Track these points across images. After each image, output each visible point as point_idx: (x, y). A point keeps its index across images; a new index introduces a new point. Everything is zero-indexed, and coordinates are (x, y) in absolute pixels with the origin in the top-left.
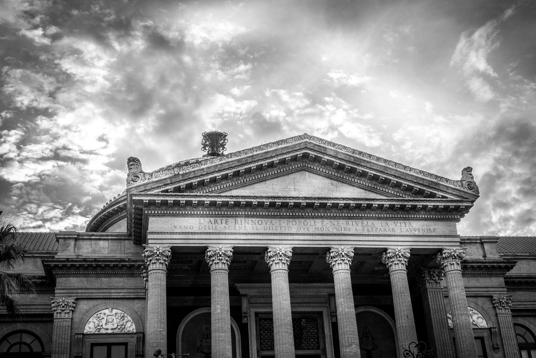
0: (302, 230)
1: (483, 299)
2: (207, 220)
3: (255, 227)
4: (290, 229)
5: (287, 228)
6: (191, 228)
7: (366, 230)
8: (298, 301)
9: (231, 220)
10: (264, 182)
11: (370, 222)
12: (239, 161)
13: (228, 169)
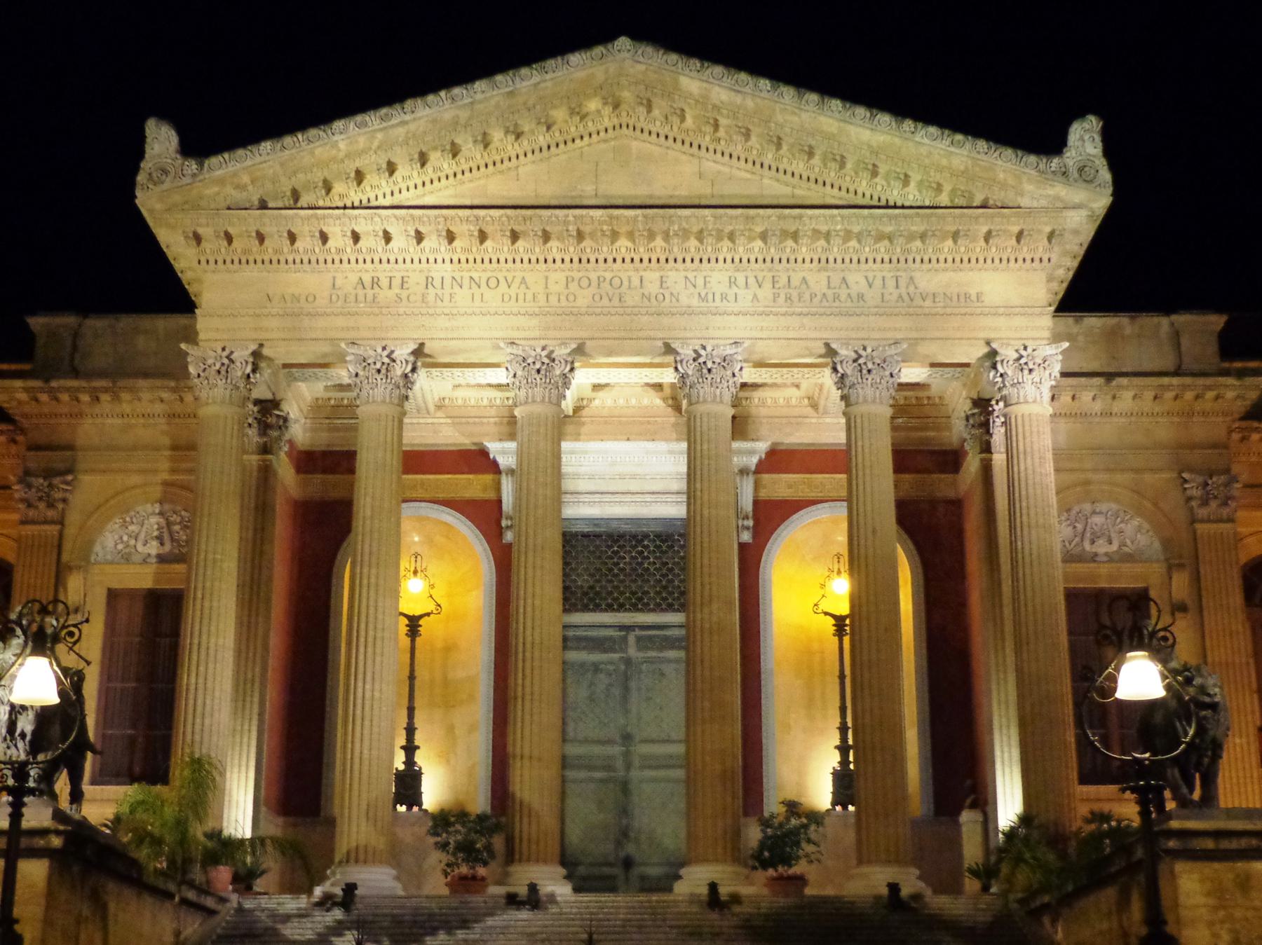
0: (605, 301)
3: (478, 298)
4: (571, 298)
5: (563, 298)
6: (311, 299)
7: (783, 296)
8: (654, 489)
10: (513, 173)
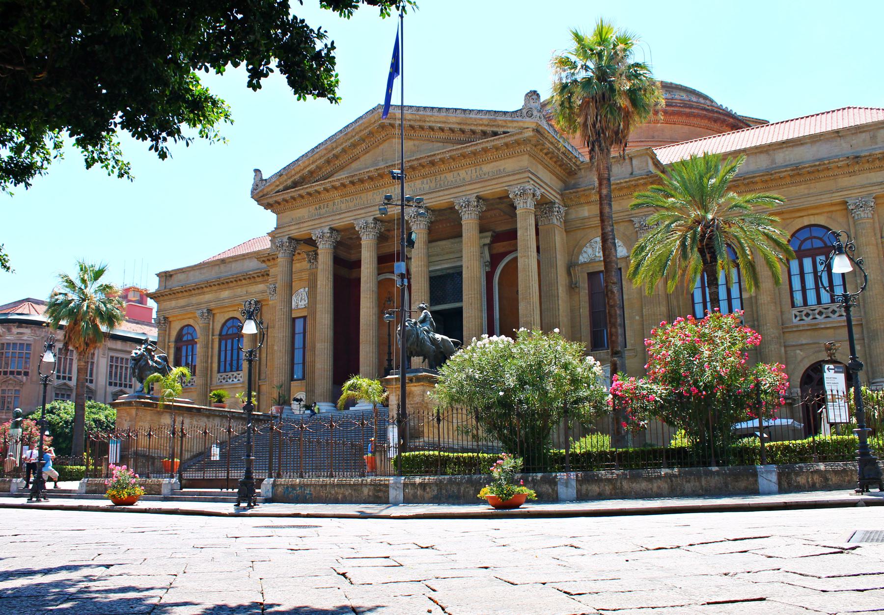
1: (626, 224)
2: (314, 207)
9: (331, 203)
11: (443, 176)
12: (326, 149)
13: (320, 158)
